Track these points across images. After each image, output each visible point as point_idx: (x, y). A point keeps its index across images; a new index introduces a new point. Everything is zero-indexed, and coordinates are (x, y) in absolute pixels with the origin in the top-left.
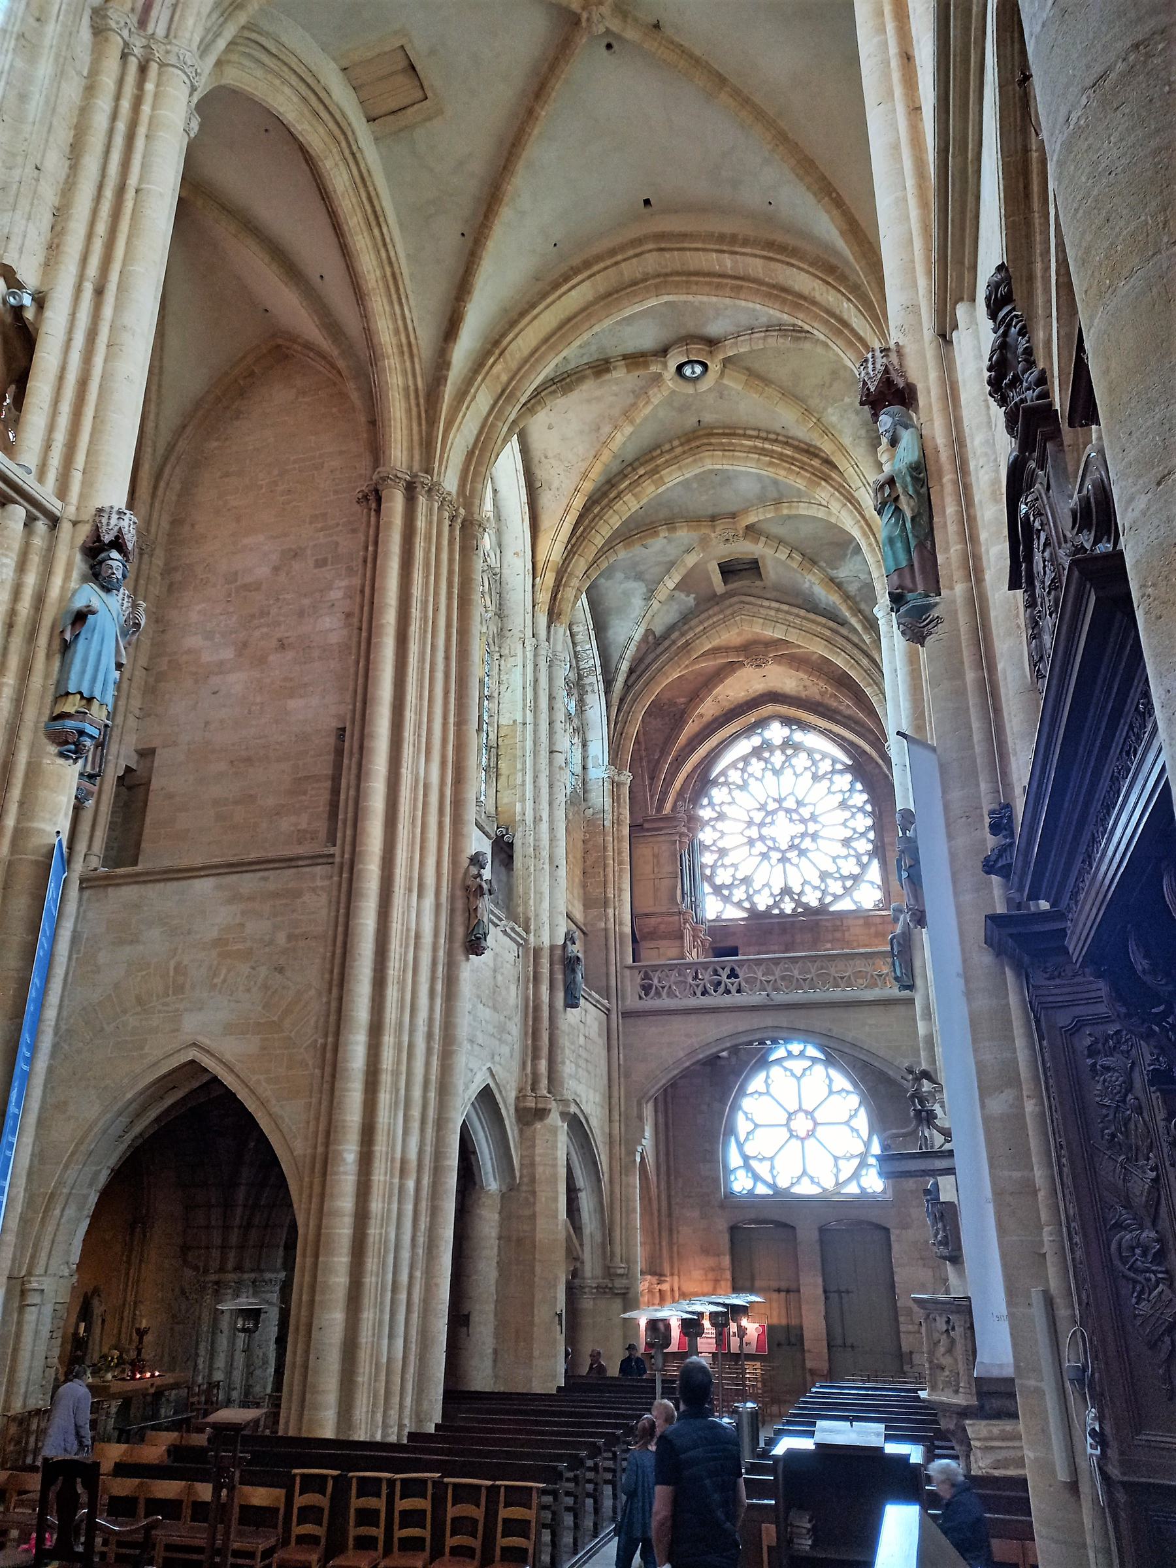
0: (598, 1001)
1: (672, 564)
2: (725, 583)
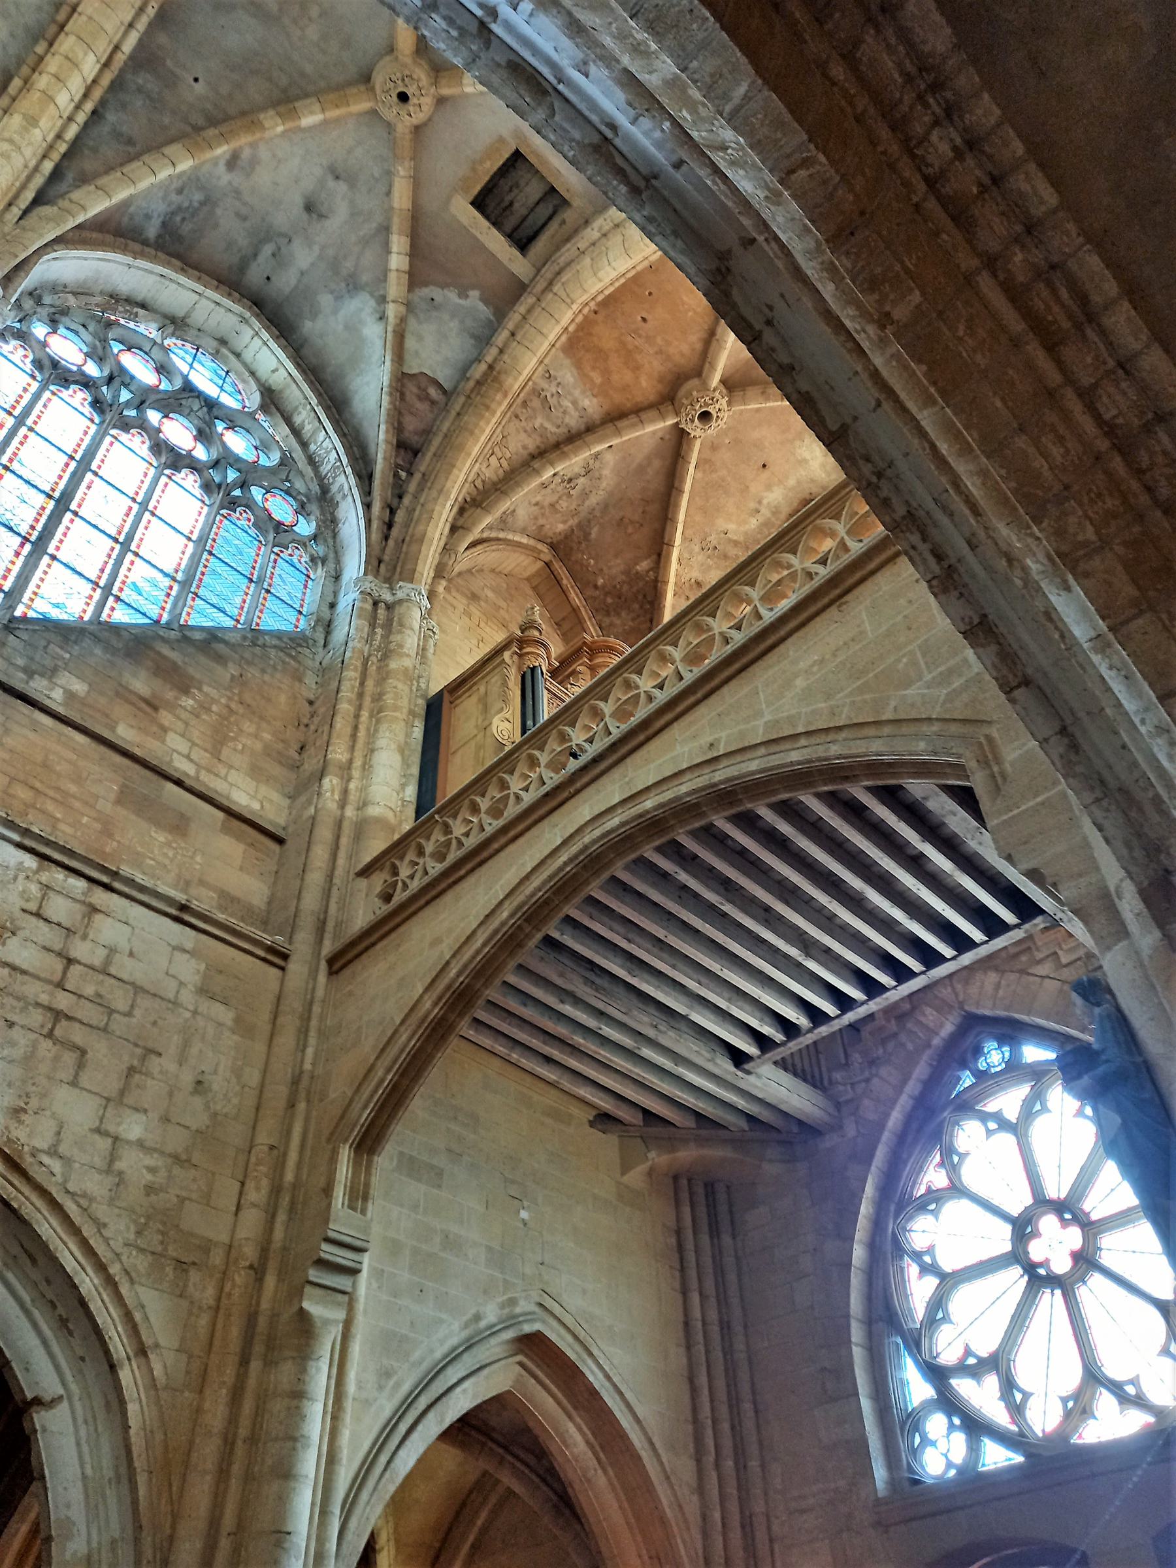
0: (183, 908)
1: (386, 229)
2: (524, 255)
